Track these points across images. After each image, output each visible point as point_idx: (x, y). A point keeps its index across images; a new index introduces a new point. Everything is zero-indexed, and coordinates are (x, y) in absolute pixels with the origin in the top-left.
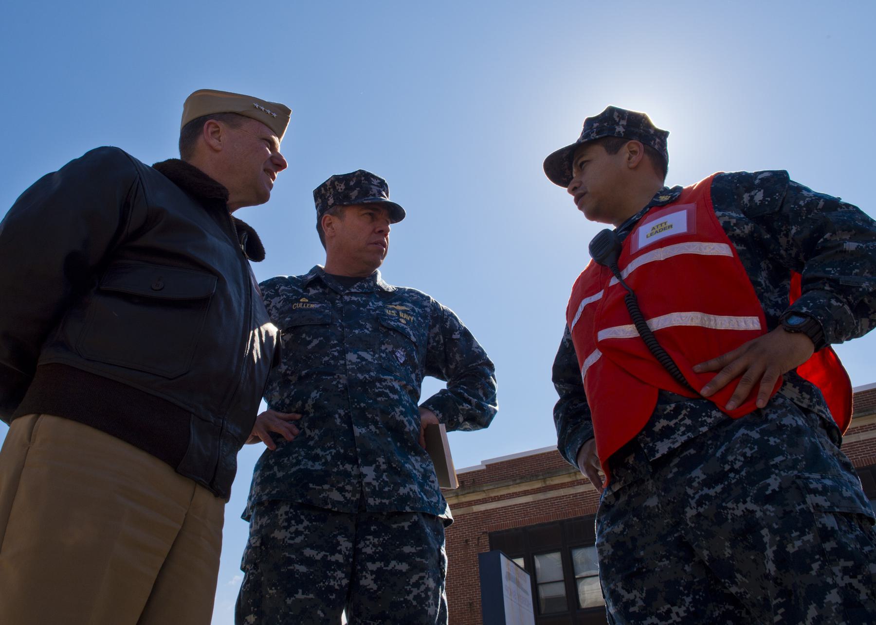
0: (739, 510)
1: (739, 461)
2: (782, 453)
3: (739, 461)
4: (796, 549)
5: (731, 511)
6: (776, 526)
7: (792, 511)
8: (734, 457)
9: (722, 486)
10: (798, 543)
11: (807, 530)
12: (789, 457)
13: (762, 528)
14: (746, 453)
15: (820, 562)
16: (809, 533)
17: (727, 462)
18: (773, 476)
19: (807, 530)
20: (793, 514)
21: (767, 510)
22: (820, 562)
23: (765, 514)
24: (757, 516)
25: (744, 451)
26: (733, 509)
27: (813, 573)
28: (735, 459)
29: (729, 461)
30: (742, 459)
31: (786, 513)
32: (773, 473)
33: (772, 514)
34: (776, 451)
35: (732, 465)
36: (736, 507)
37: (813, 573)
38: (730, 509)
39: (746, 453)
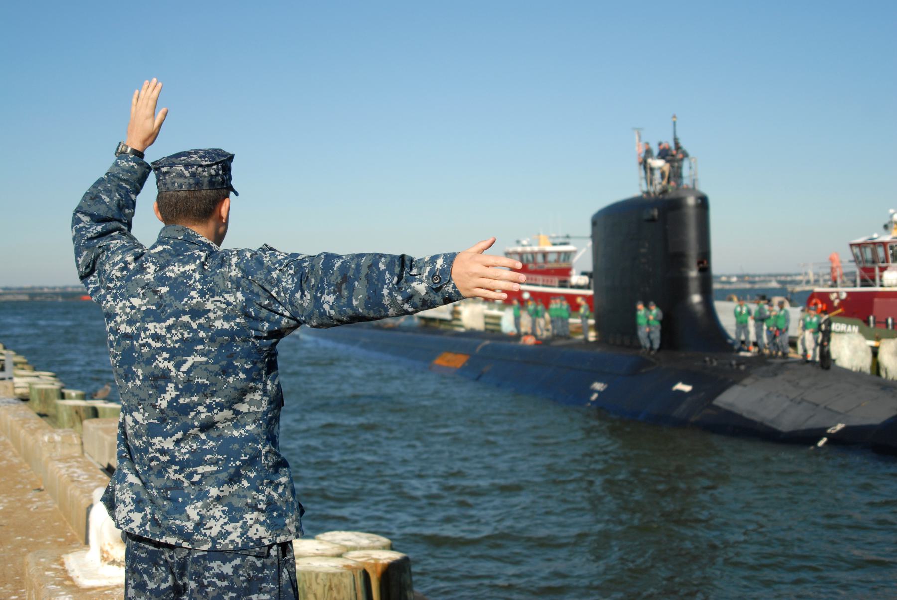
0: (163, 365)
1: (178, 336)
2: (203, 343)
3: (178, 336)
4: (186, 403)
5: (158, 362)
6: (180, 387)
7: (192, 381)
8: (176, 332)
9: (161, 345)
10: (188, 400)
11: (196, 394)
12: (207, 347)
13: (171, 383)
14: (184, 334)
15: (196, 413)
16: (196, 396)
17: (170, 332)
18: (193, 356)
19: (196, 394)
20: (192, 383)
21: (180, 375)
22: (196, 413)
23: (177, 376)
24: (171, 375)
25: (184, 332)
26: (160, 362)
27: (190, 417)
28: (176, 334)
29: (171, 332)
30: (181, 336)
31: (189, 381)
32: (193, 354)
33: (182, 379)
34: (201, 341)
35: (172, 336)
36: (162, 362)
37: (190, 417)
38: (158, 361)
39: (184, 334)
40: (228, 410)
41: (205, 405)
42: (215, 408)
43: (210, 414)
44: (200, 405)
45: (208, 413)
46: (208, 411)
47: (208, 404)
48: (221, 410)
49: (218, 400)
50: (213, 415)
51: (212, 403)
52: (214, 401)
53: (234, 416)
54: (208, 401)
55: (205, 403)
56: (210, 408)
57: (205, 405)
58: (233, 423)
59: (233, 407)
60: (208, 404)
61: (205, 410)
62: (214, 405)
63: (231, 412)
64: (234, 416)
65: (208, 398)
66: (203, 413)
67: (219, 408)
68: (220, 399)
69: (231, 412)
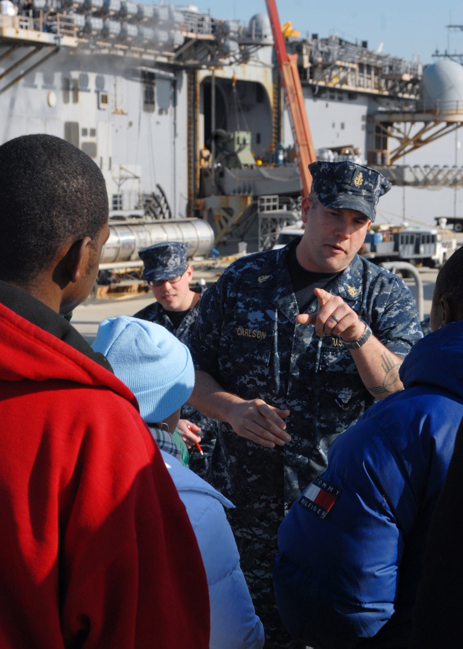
40: (260, 312)
41: (244, 302)
42: (252, 307)
43: (245, 311)
44: (241, 301)
45: (245, 309)
46: (245, 308)
47: (247, 301)
48: (255, 310)
49: (256, 300)
50: (248, 312)
51: (251, 301)
52: (253, 300)
53: (263, 320)
54: (248, 299)
55: (245, 301)
56: (247, 306)
57: (244, 302)
58: (260, 327)
59: (266, 311)
60: (247, 301)
61: (243, 306)
62: (252, 303)
63: (263, 315)
64: (263, 320)
65: (248, 297)
66: (241, 308)
67: (254, 307)
68: (258, 300)
69: (263, 315)
